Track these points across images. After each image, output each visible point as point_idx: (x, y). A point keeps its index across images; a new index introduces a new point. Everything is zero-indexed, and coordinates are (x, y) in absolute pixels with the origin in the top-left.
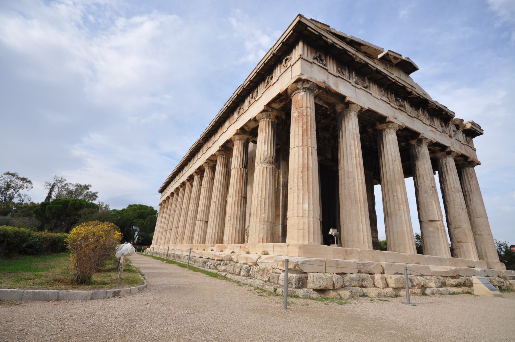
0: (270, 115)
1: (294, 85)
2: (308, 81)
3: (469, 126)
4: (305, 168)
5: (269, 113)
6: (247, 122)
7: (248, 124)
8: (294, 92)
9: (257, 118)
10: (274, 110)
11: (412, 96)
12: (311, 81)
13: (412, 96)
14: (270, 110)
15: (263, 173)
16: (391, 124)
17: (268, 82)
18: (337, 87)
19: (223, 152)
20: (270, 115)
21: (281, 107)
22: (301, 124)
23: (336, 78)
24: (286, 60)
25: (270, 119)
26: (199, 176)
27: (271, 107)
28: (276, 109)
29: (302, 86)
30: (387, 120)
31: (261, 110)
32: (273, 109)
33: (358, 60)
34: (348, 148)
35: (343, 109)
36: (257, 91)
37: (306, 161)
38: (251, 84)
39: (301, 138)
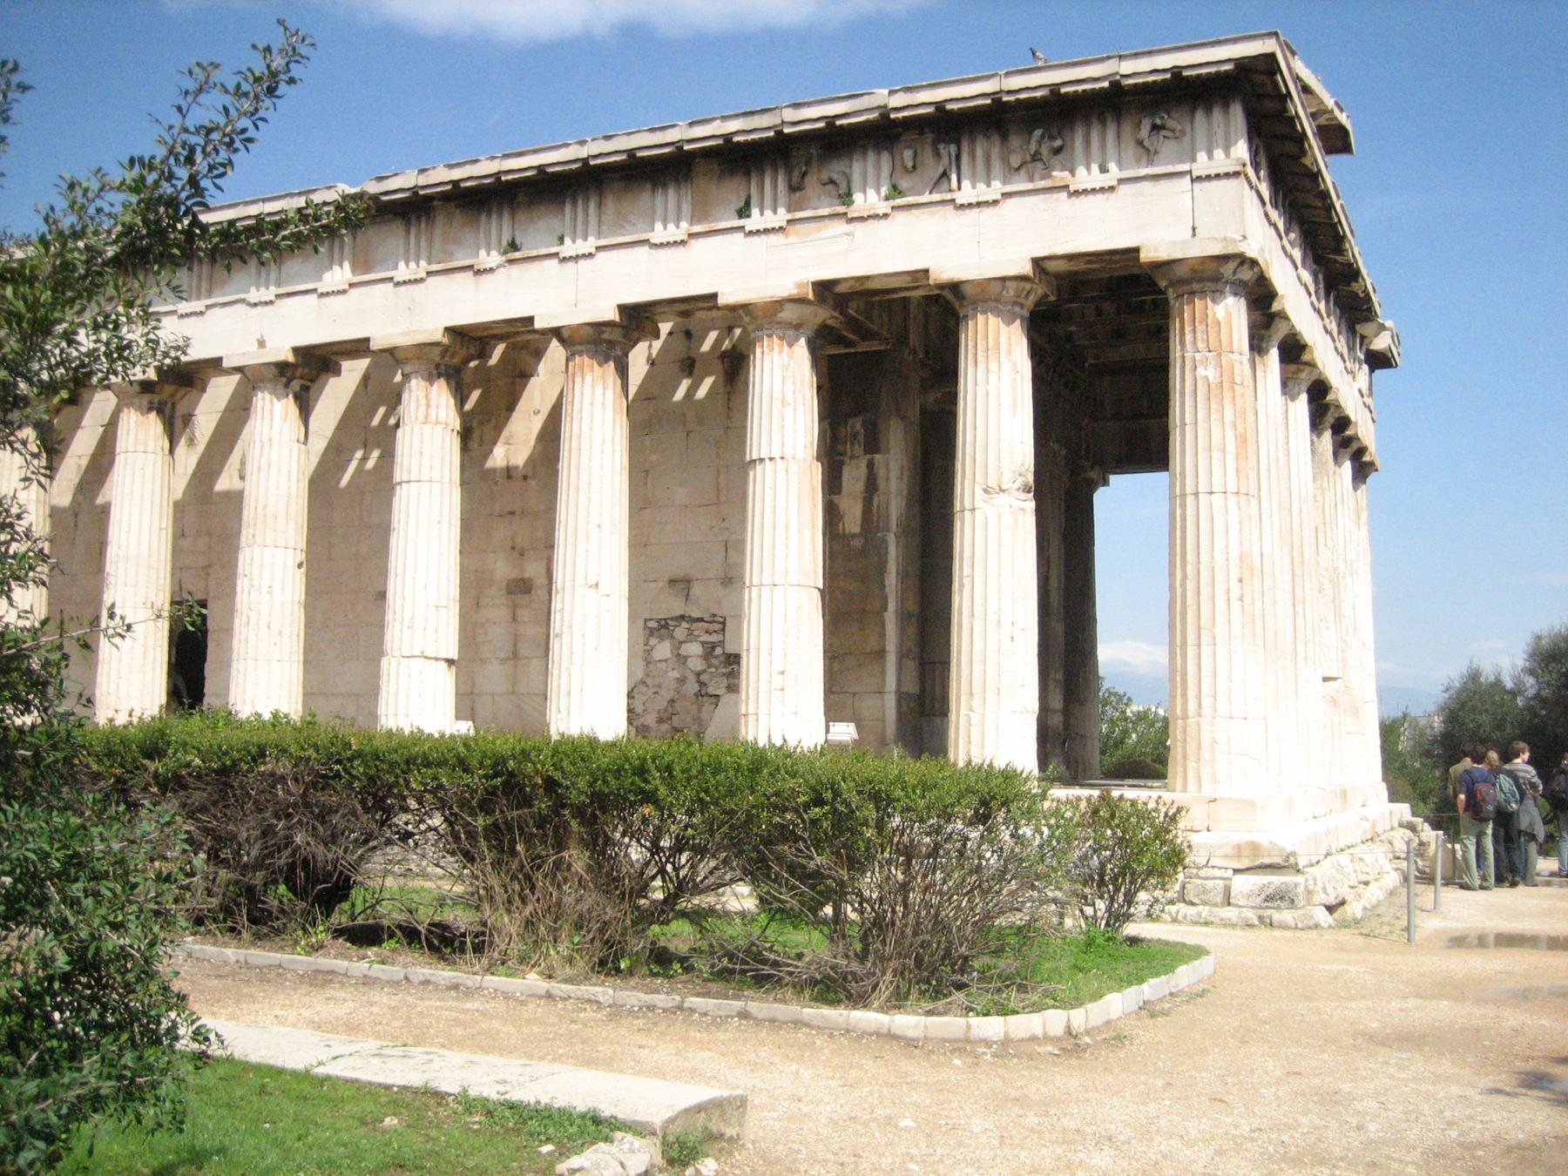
1: (1213, 265)
2: (1254, 263)
3: (1381, 343)
5: (1028, 286)
8: (1201, 280)
9: (968, 290)
11: (1339, 258)
13: (1339, 258)
16: (1308, 369)
17: (1037, 153)
19: (616, 335)
22: (1229, 415)
24: (1155, 128)
25: (1022, 306)
26: (296, 385)
29: (1234, 273)
30: (1306, 357)
31: (1012, 273)
33: (1307, 161)
34: (1263, 474)
36: (958, 157)
39: (1231, 466)
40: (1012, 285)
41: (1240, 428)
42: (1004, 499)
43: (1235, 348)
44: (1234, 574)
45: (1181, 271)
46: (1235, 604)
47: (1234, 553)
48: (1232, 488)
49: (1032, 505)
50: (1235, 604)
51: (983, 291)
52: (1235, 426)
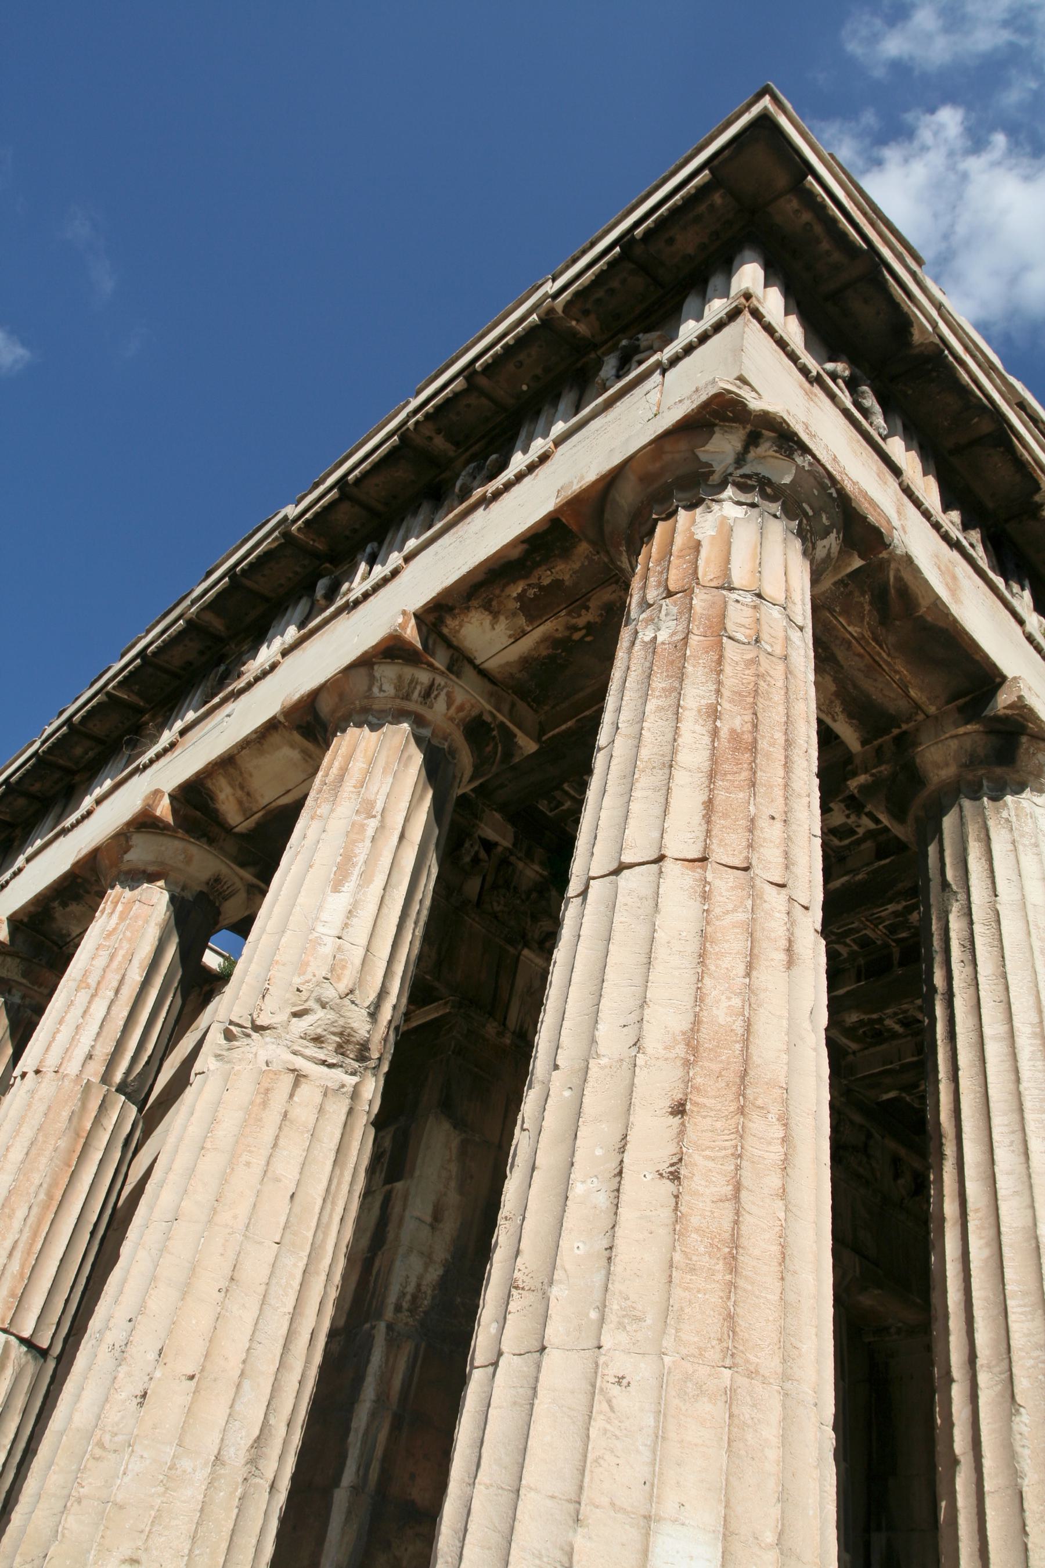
0: (428, 694)
4: (713, 1069)
5: (424, 677)
6: (246, 744)
7: (249, 762)
9: (325, 706)
10: (469, 672)
12: (805, 450)
14: (439, 662)
15: (250, 1120)
18: (953, 592)
20: (428, 694)
21: (525, 662)
23: (944, 546)
27: (449, 645)
28: (482, 673)
29: (740, 460)
32: (460, 660)
35: (972, 761)
37: (723, 1009)
38: (345, 514)
40: (388, 673)
41: (735, 720)
42: (261, 1050)
43: (739, 576)
44: (658, 1083)
45: (627, 495)
46: (644, 1188)
47: (666, 1021)
48: (682, 841)
49: (371, 1088)
50: (644, 1188)
51: (341, 696)
52: (714, 713)
